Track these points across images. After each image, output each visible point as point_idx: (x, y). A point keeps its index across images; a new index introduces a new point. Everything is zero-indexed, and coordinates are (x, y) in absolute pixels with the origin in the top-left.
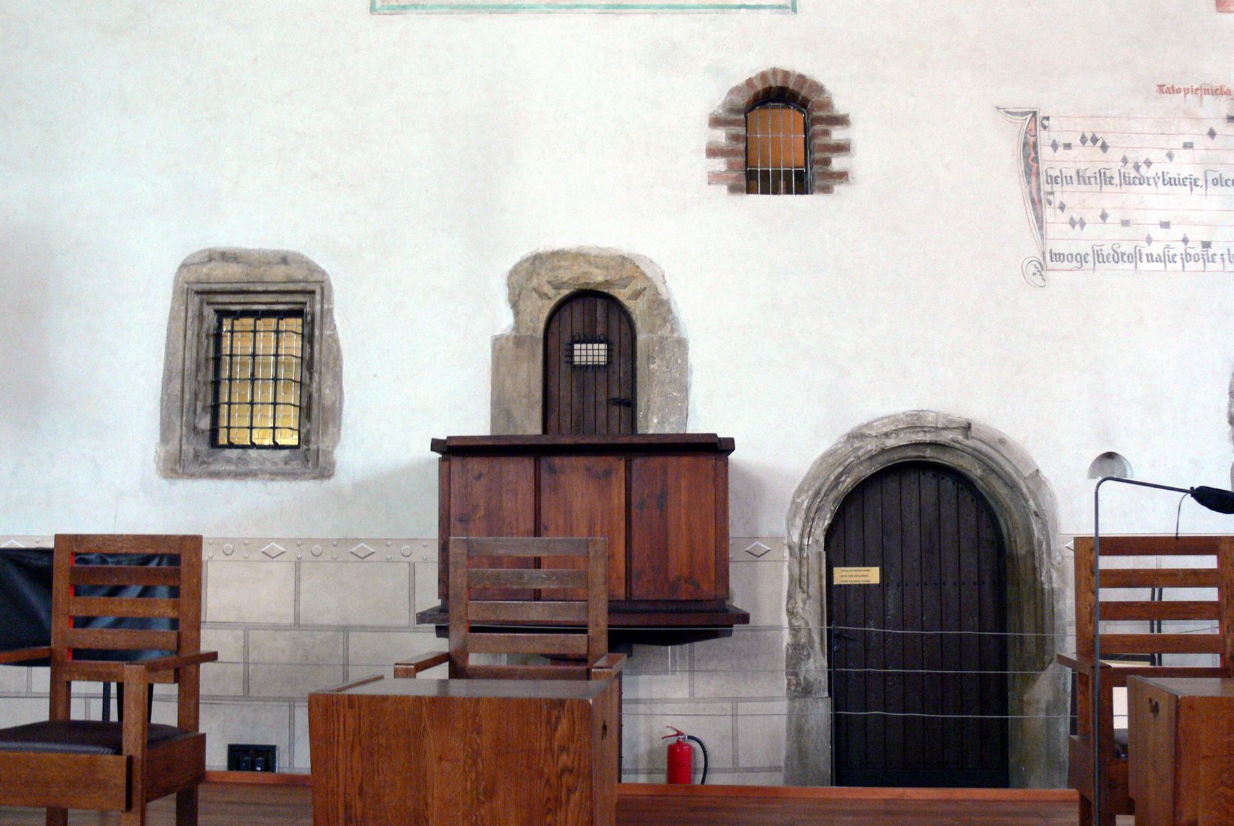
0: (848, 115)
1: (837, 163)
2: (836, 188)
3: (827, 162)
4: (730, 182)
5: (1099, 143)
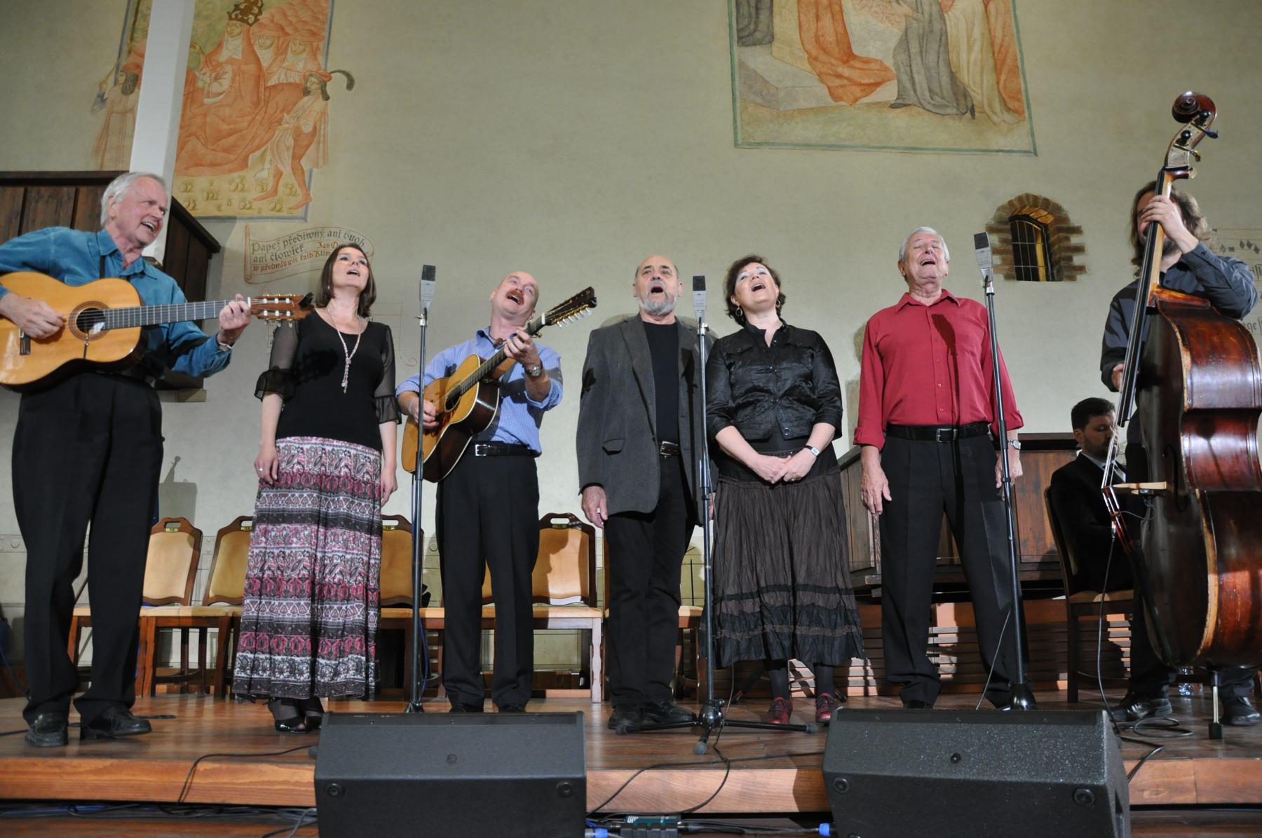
0: (1080, 227)
1: (1077, 260)
2: (1079, 277)
3: (1070, 259)
4: (1005, 272)
5: (1253, 247)
